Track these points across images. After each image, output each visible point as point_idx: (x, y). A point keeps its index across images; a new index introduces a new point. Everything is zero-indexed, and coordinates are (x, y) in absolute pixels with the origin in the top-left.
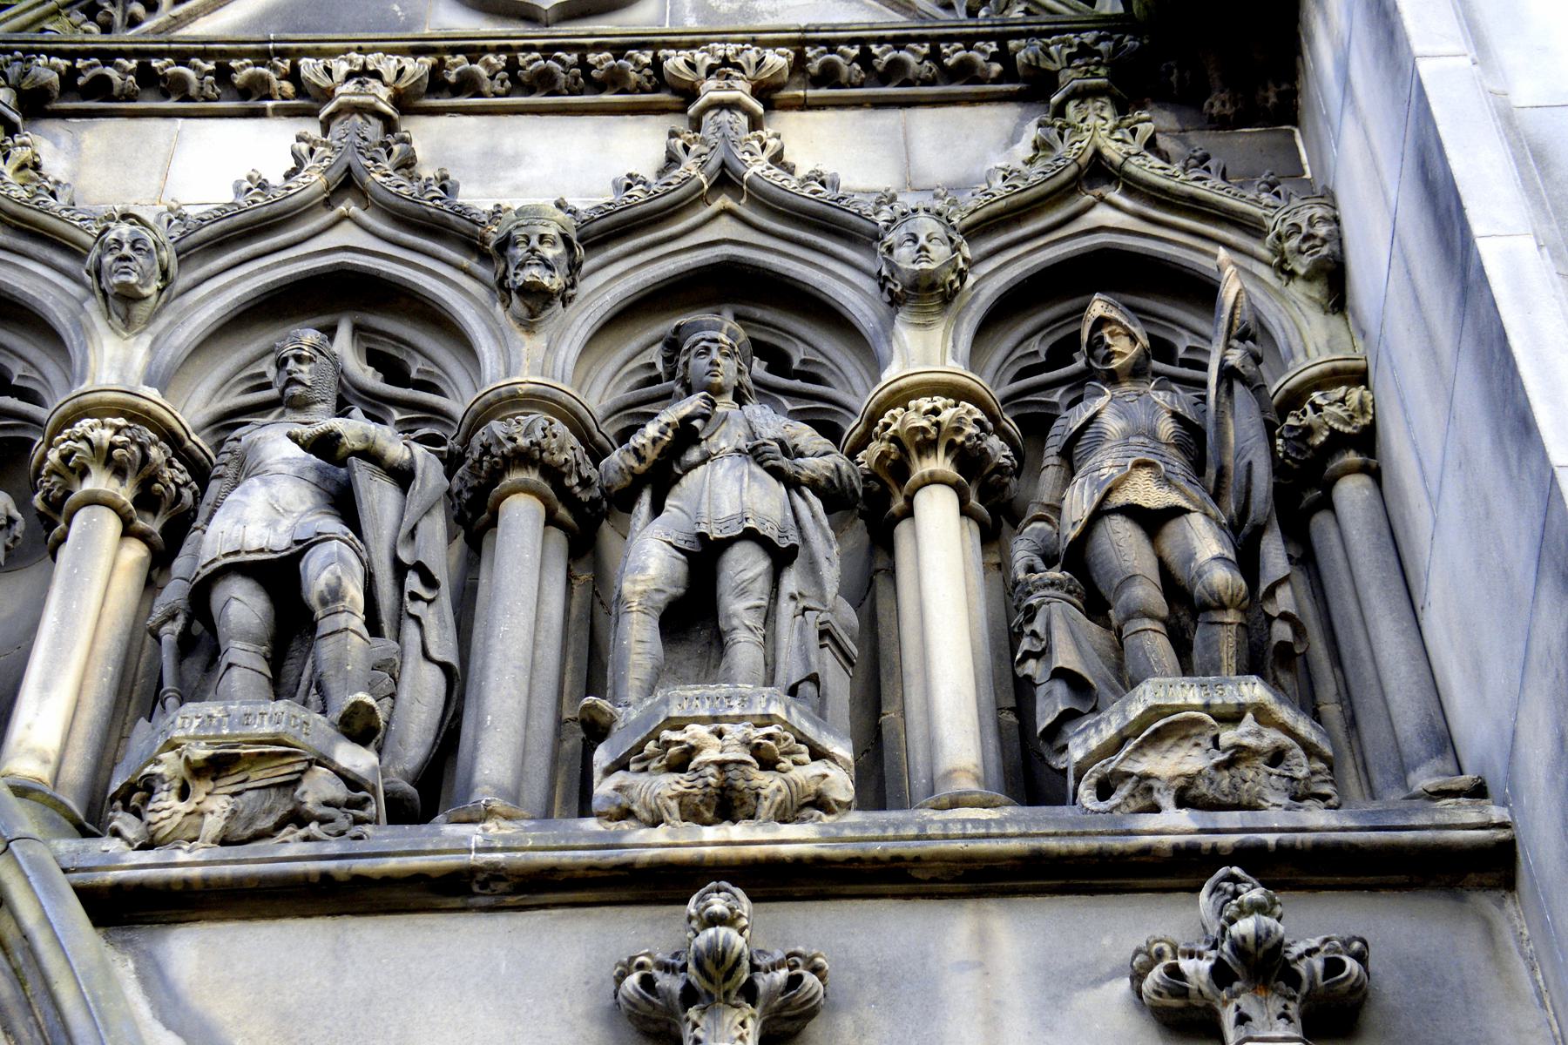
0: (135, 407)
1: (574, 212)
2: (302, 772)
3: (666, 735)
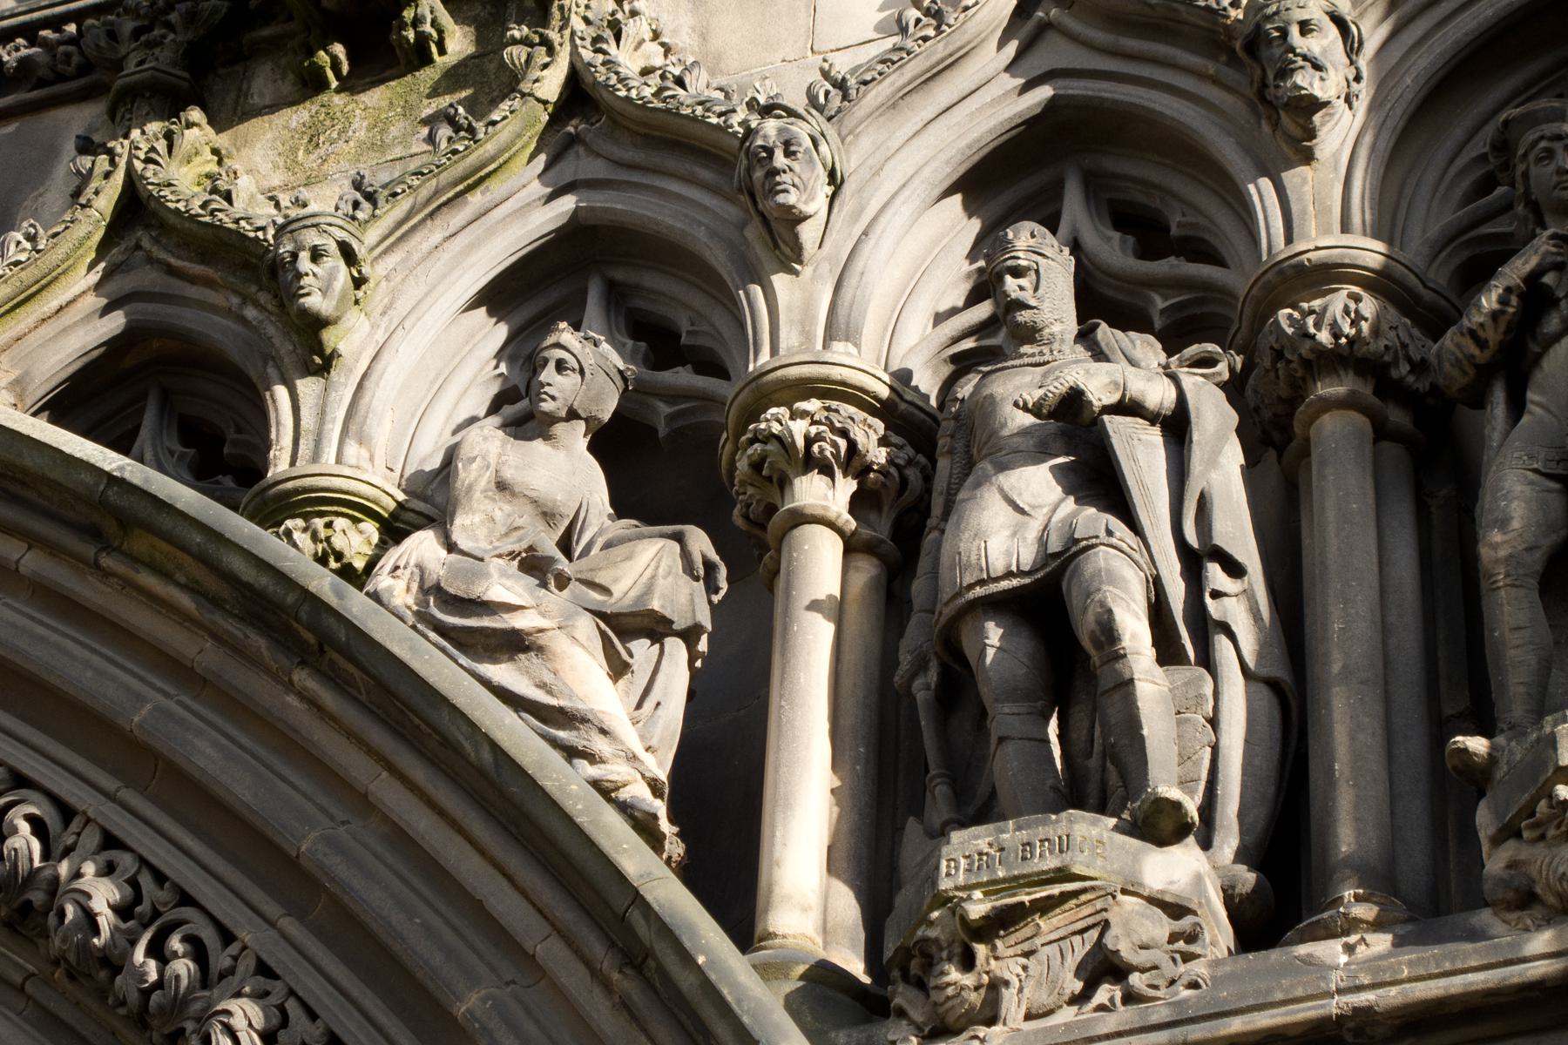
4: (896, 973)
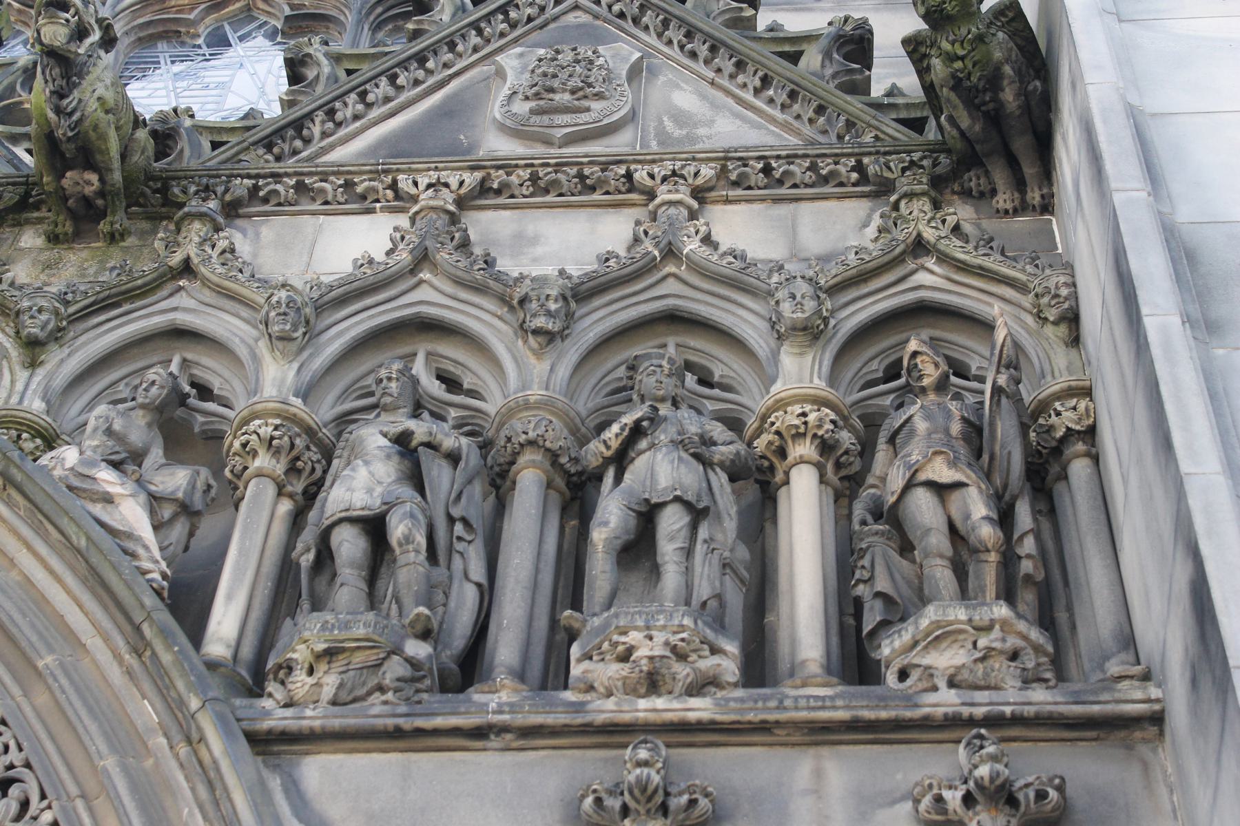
0: (287, 411)
1: (569, 278)
2: (384, 659)
3: (615, 638)
4: (271, 676)
